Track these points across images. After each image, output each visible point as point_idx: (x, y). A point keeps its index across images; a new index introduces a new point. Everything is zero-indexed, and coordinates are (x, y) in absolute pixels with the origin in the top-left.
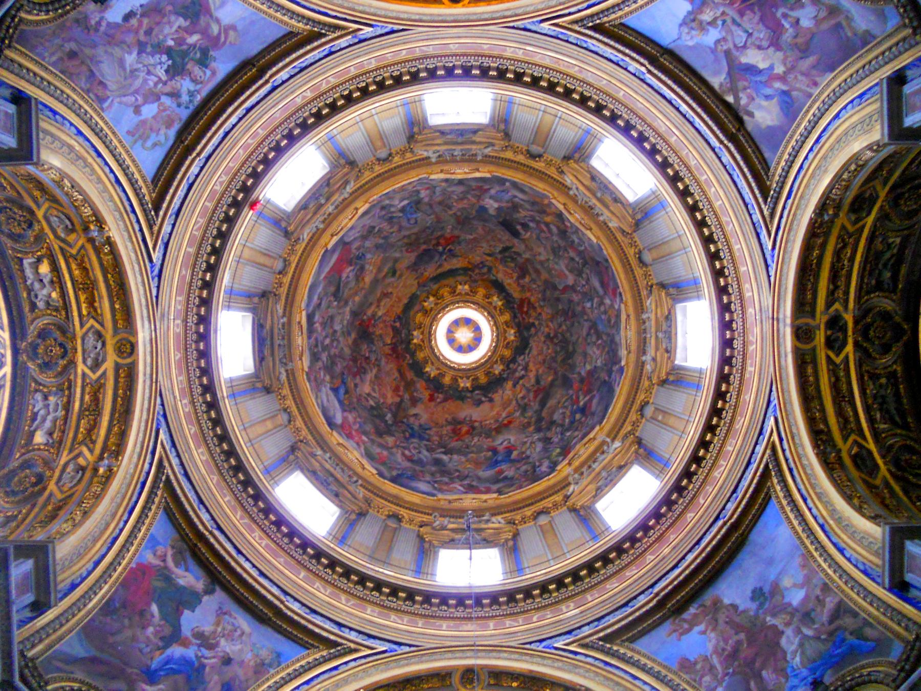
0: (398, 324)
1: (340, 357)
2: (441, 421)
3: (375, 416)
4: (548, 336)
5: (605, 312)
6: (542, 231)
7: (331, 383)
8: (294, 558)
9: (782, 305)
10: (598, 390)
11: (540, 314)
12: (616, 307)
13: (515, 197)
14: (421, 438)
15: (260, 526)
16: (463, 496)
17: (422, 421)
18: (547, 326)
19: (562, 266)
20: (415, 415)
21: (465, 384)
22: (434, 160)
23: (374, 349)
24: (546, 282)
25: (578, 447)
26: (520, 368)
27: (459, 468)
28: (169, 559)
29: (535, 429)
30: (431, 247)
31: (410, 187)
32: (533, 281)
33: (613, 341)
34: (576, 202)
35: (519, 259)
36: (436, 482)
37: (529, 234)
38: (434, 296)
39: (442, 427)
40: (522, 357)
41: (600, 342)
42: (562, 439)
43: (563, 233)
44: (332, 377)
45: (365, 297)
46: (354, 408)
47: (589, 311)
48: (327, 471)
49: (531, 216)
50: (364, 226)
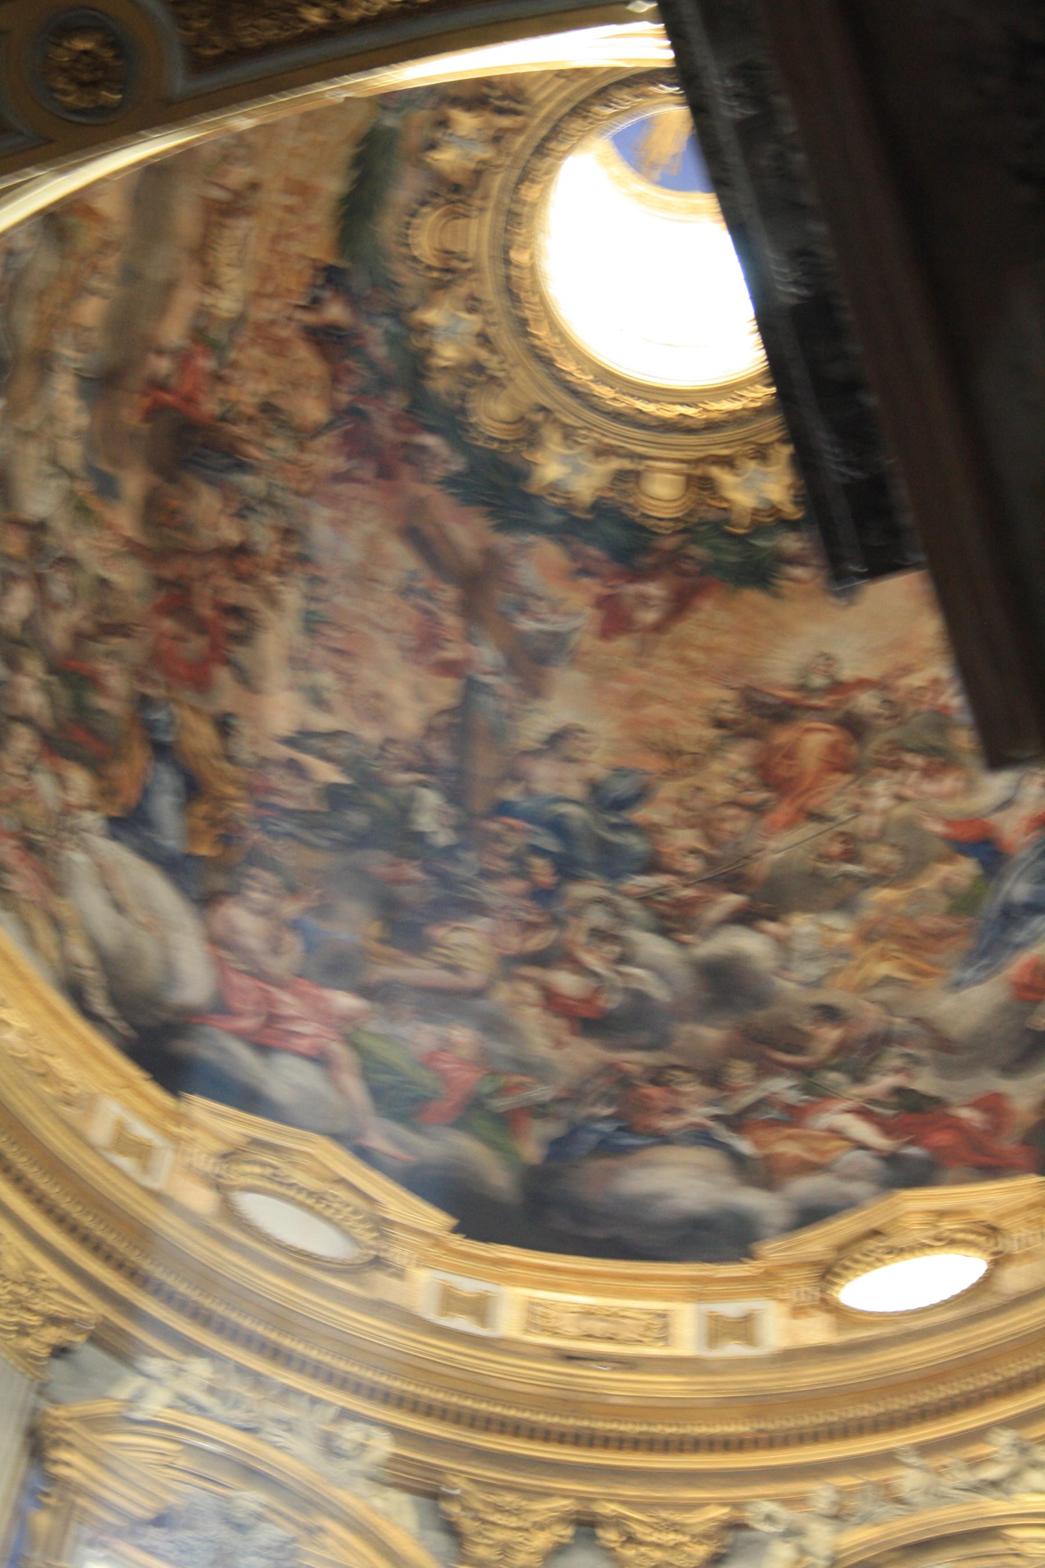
0: (336, 312)
3: (361, 841)
7: (107, 792)
17: (597, 767)
36: (737, 1122)
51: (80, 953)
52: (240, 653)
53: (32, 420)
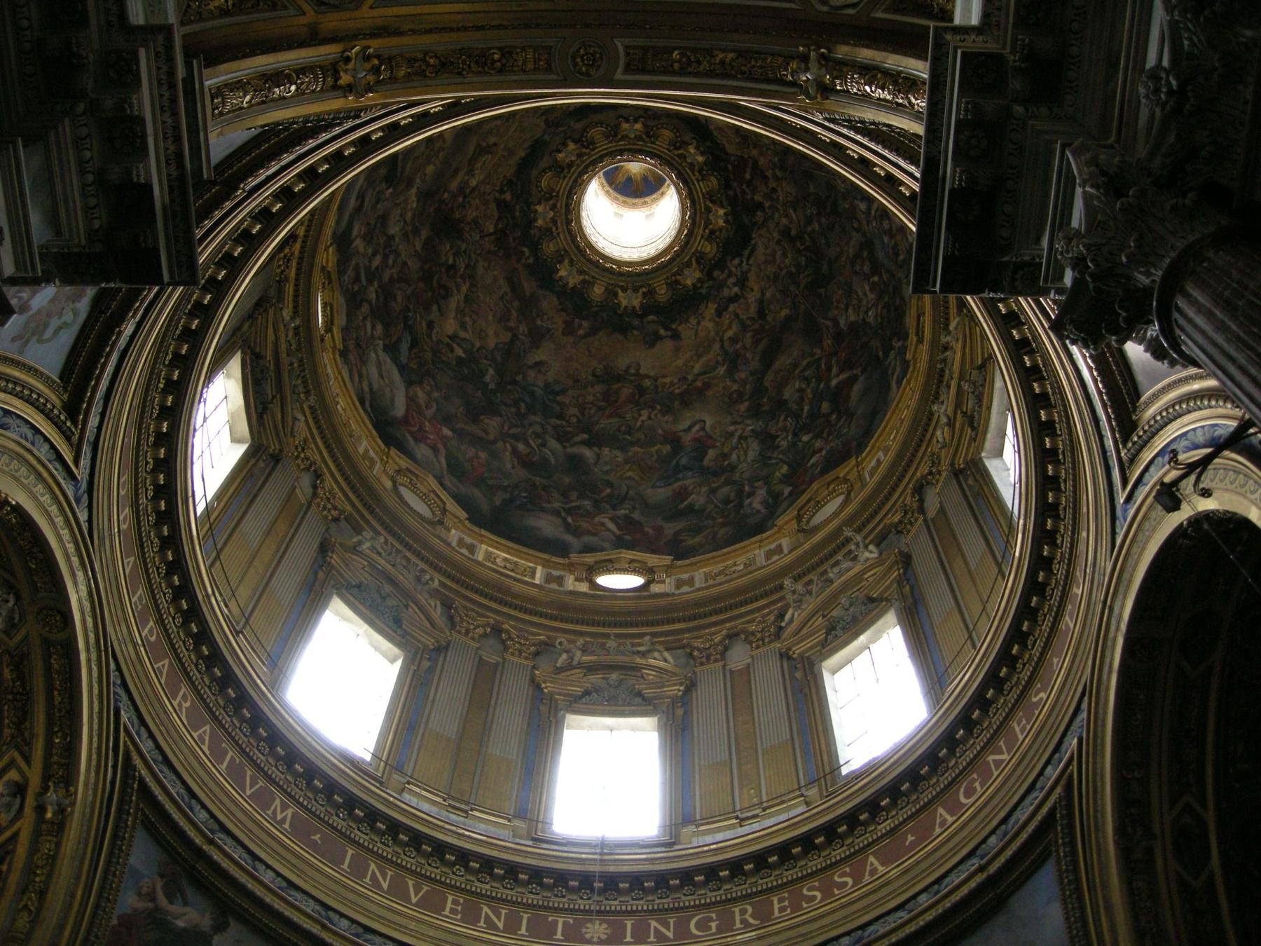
0: (508, 196)
4: (785, 233)
9: (1120, 597)
11: (774, 190)
15: (281, 787)
17: (550, 377)
20: (539, 364)
21: (629, 300)
23: (464, 247)
25: (815, 486)
26: (732, 280)
28: (160, 895)
29: (749, 409)
36: (569, 511)
38: (576, 141)
39: (585, 387)
40: (737, 261)
41: (876, 279)
42: (794, 444)
44: (386, 326)
51: (366, 388)
53: (402, 199)
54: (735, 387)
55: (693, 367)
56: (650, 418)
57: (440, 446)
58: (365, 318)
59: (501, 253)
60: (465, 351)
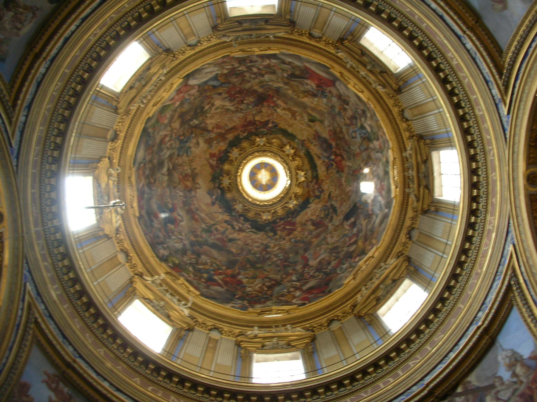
0: (270, 125)
1: (243, 80)
2: (194, 165)
4: (267, 246)
5: (289, 292)
6: (350, 239)
7: (222, 75)
8: (80, 63)
10: (227, 290)
11: (284, 239)
12: (294, 301)
13: (377, 216)
14: (181, 148)
15: (104, 33)
16: (135, 188)
17: (193, 149)
18: (275, 246)
19: (324, 255)
20: (198, 143)
21: (226, 182)
22: (404, 154)
23: (250, 107)
24: (310, 243)
25: (182, 279)
26: (241, 225)
27: (157, 182)
30: (334, 150)
31: (381, 133)
32: (311, 232)
33: (267, 299)
34: (375, 268)
35: (328, 220)
36: (145, 164)
37: (348, 228)
38: (295, 153)
39: (190, 166)
40: (249, 226)
41: (266, 289)
42: (186, 264)
43: (350, 256)
44: (226, 75)
45: (291, 99)
46: (202, 94)
47: (289, 278)
48: (150, 79)
49: (362, 229)
50: (349, 97)
51: (205, 67)
52: (228, 99)
53: (280, 80)
54: (199, 233)
55: (202, 213)
56: (181, 196)
57: (173, 101)
58: (233, 65)
59: (245, 123)
60: (207, 110)
